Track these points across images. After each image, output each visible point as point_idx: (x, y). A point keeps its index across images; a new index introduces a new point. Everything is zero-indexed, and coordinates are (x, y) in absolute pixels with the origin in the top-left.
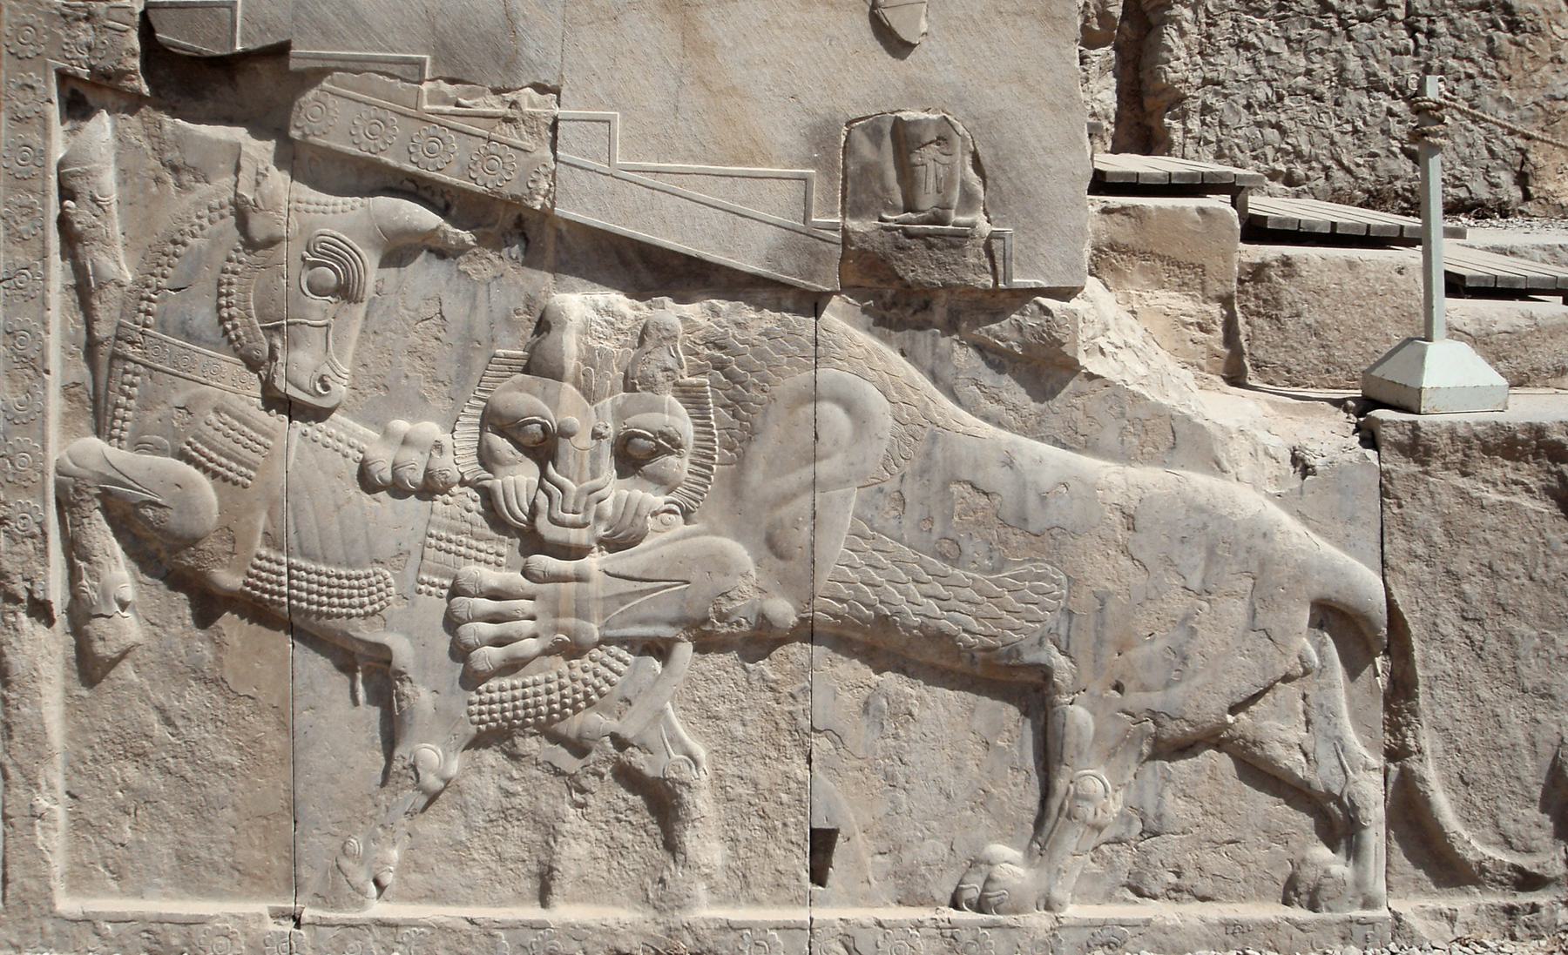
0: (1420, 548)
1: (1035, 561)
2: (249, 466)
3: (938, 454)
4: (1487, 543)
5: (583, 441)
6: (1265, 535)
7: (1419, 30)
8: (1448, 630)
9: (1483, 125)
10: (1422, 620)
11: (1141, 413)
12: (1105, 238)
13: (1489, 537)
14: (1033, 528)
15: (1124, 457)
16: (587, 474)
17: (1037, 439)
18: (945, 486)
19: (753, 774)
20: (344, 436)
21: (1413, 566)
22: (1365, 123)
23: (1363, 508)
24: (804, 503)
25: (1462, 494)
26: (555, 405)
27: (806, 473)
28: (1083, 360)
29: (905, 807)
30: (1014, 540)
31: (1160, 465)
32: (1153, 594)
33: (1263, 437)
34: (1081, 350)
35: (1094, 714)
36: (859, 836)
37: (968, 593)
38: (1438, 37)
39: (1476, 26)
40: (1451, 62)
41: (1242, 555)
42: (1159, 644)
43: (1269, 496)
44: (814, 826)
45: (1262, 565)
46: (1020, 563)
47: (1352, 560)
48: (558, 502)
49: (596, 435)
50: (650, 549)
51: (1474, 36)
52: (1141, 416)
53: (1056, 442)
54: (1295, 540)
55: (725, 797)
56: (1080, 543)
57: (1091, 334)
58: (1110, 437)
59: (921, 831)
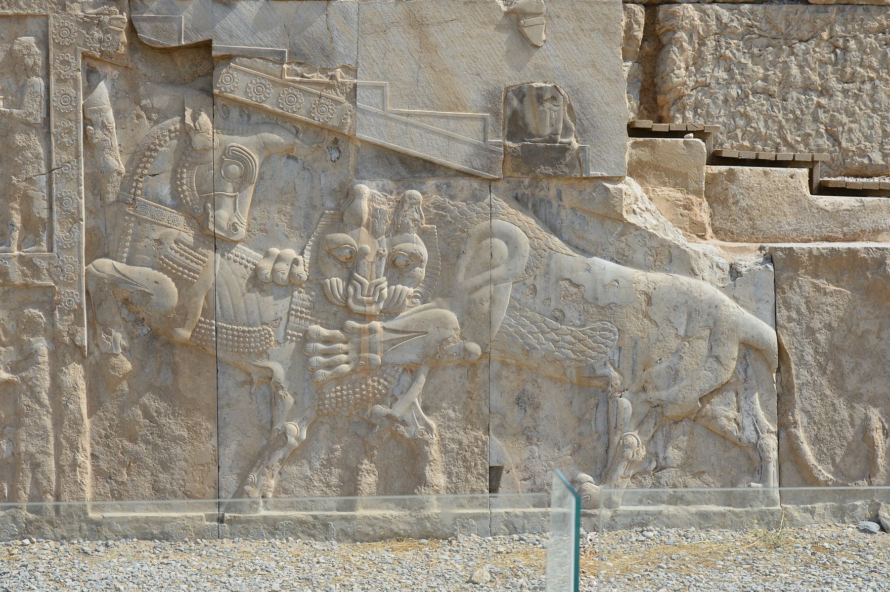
0: (794, 315)
1: (603, 320)
2: (195, 272)
3: (553, 265)
4: (828, 312)
5: (371, 258)
6: (716, 307)
7: (836, 47)
8: (809, 359)
9: (880, 113)
10: (796, 354)
11: (655, 244)
12: (635, 158)
13: (829, 309)
14: (601, 303)
15: (647, 268)
16: (374, 275)
17: (601, 257)
18: (557, 281)
19: (460, 437)
20: (245, 257)
21: (792, 324)
22: (802, 111)
23: (766, 294)
24: (486, 291)
25: (815, 286)
26: (358, 240)
27: (486, 275)
28: (625, 215)
29: (537, 454)
30: (591, 310)
31: (663, 272)
32: (661, 338)
33: (716, 258)
34: (624, 209)
35: (632, 403)
36: (514, 470)
37: (569, 338)
38: (850, 52)
39: (875, 44)
40: (858, 69)
41: (705, 317)
42: (664, 364)
43: (718, 287)
44: (491, 465)
45: (715, 323)
46: (595, 322)
47: (760, 321)
48: (359, 290)
49: (378, 254)
50: (407, 316)
51: (873, 51)
52: (654, 245)
53: (612, 260)
54: (732, 310)
55: (445, 450)
56: (624, 311)
57: (629, 202)
58: (639, 256)
59: (545, 467)
